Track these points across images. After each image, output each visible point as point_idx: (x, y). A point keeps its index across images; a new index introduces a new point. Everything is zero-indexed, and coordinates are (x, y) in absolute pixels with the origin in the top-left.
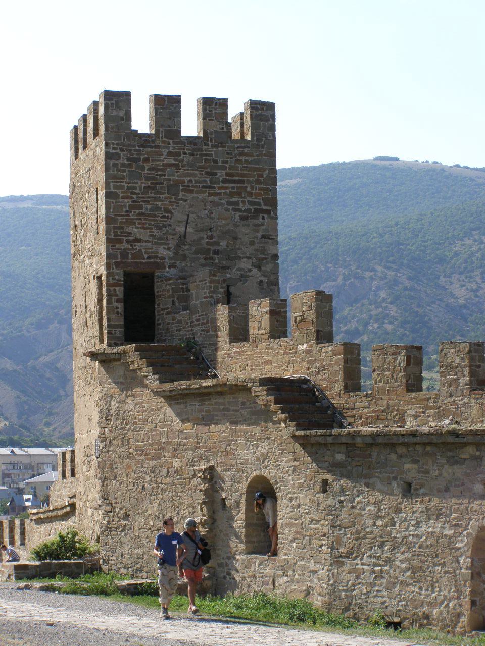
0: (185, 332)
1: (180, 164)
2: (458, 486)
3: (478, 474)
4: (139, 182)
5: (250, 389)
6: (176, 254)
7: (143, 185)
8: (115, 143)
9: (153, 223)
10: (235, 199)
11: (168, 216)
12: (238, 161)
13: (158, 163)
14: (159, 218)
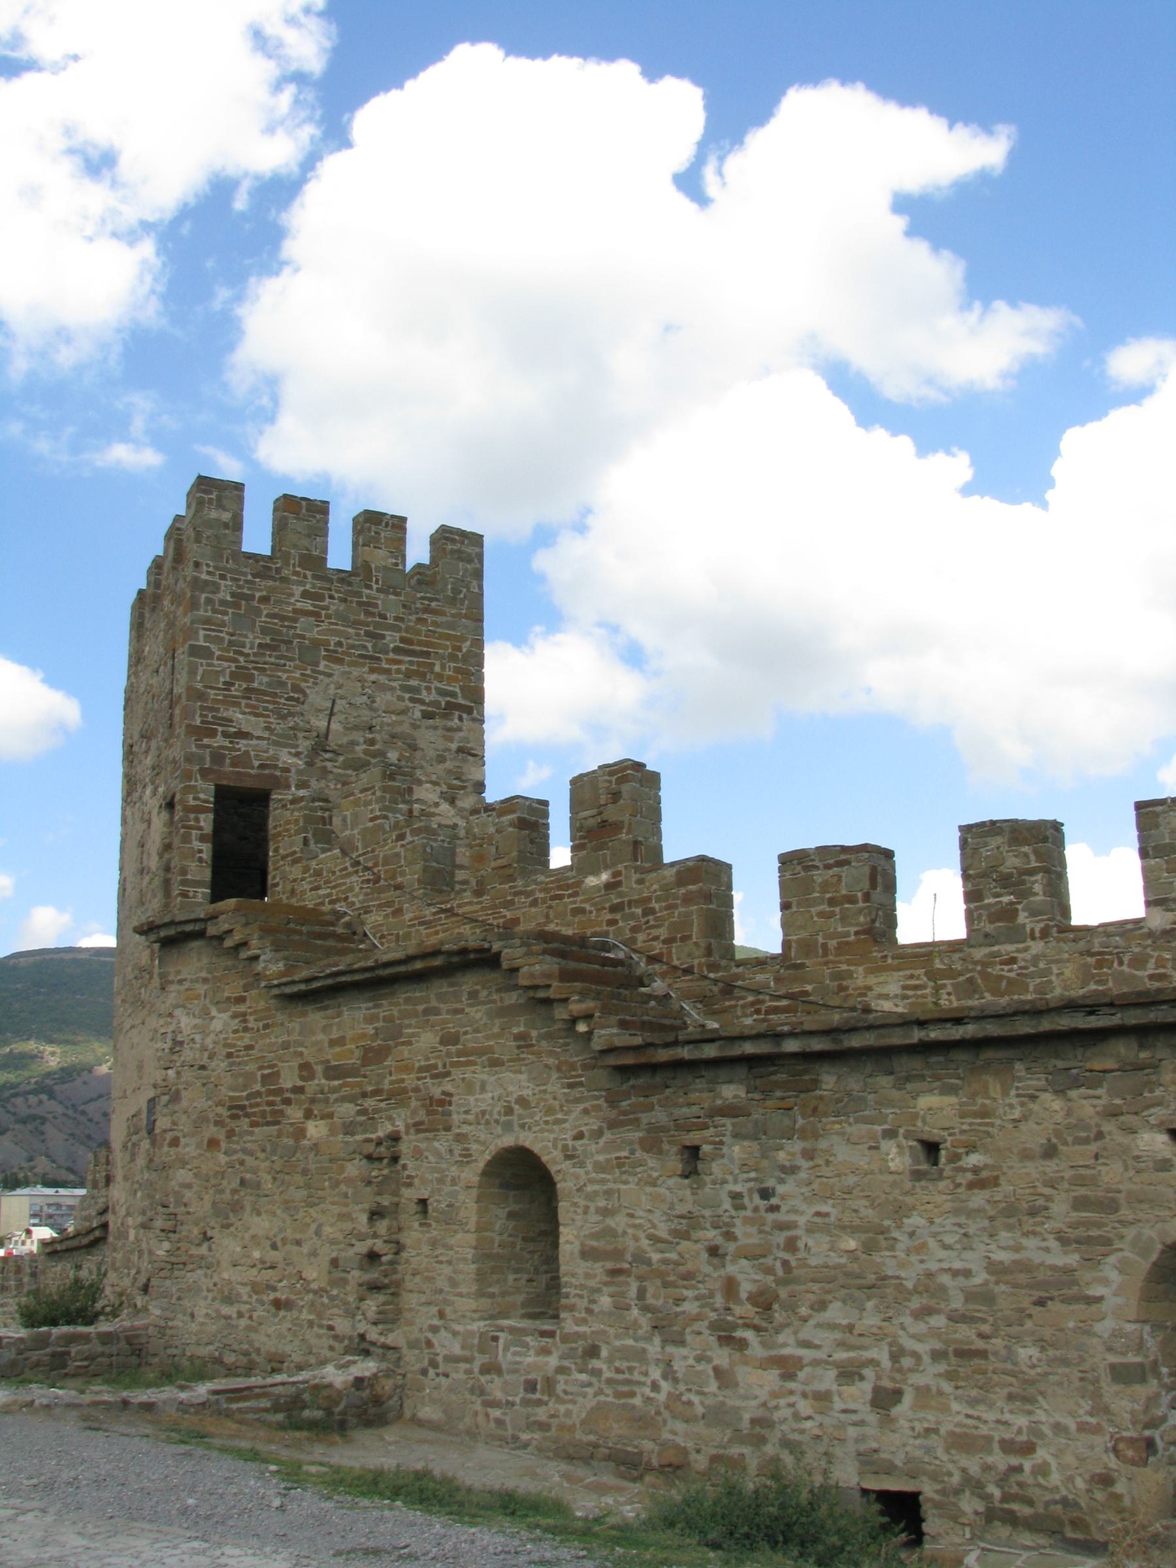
0: (329, 891)
1: (323, 612)
2: (1086, 1141)
3: (1148, 1107)
4: (251, 636)
5: (498, 955)
6: (310, 764)
7: (258, 641)
8: (211, 564)
9: (271, 707)
10: (414, 682)
12: (419, 620)
13: (284, 606)
14: (283, 701)
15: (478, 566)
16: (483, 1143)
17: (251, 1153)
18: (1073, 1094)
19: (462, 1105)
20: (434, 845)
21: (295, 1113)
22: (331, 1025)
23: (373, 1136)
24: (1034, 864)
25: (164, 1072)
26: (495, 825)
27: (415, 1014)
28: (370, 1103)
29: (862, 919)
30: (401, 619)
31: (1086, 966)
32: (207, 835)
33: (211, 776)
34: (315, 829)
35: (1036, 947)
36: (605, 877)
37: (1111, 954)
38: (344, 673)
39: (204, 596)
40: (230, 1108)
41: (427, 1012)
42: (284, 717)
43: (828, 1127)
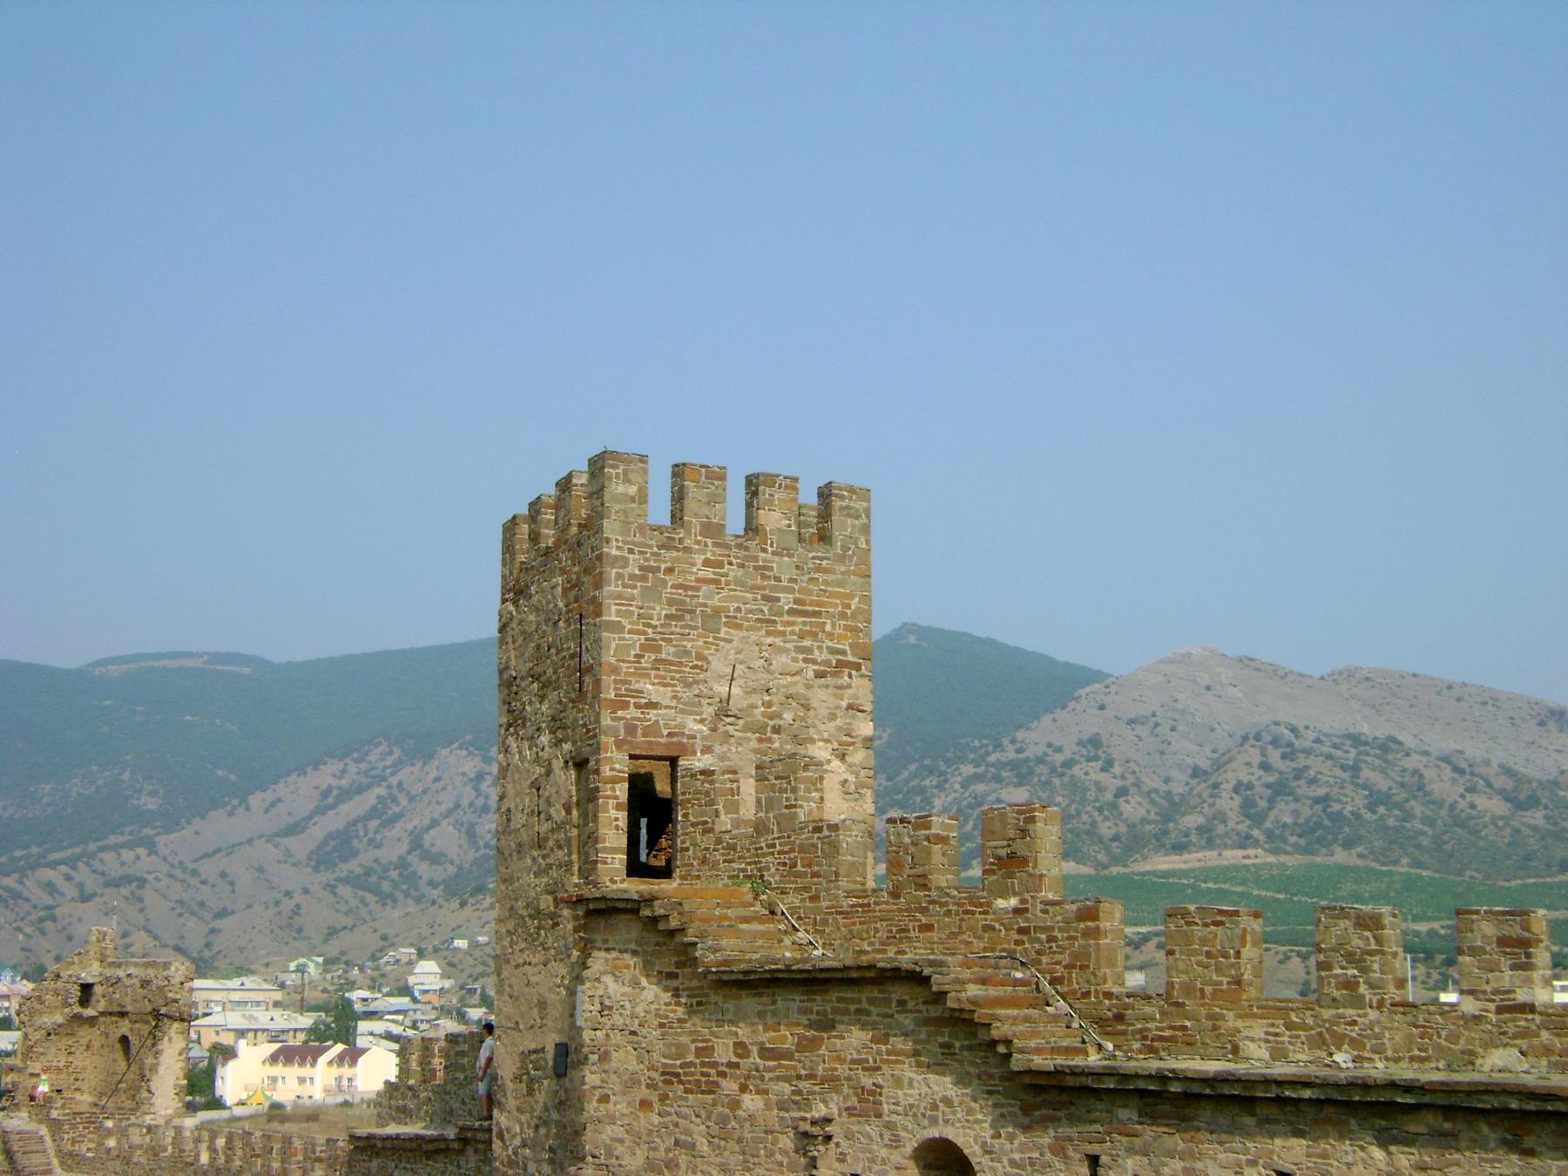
3: (1448, 1166)
4: (658, 608)
5: (928, 979)
6: (714, 730)
7: (664, 613)
9: (678, 676)
10: (807, 643)
11: (702, 666)
12: (812, 580)
14: (688, 669)
15: (866, 521)
16: (911, 1132)
17: (685, 1117)
18: (1393, 1148)
19: (892, 1097)
20: (849, 839)
21: (730, 1086)
22: (766, 1012)
23: (808, 1115)
24: (1374, 947)
25: (593, 1032)
26: (910, 836)
27: (846, 1012)
28: (805, 1085)
29: (1233, 972)
31: (1410, 1035)
32: (623, 803)
33: (625, 747)
34: (726, 800)
35: (1373, 1015)
36: (1014, 902)
37: (1431, 1028)
38: (743, 638)
39: (614, 571)
40: (663, 1073)
41: (858, 1011)
42: (689, 686)
43: (1204, 1151)
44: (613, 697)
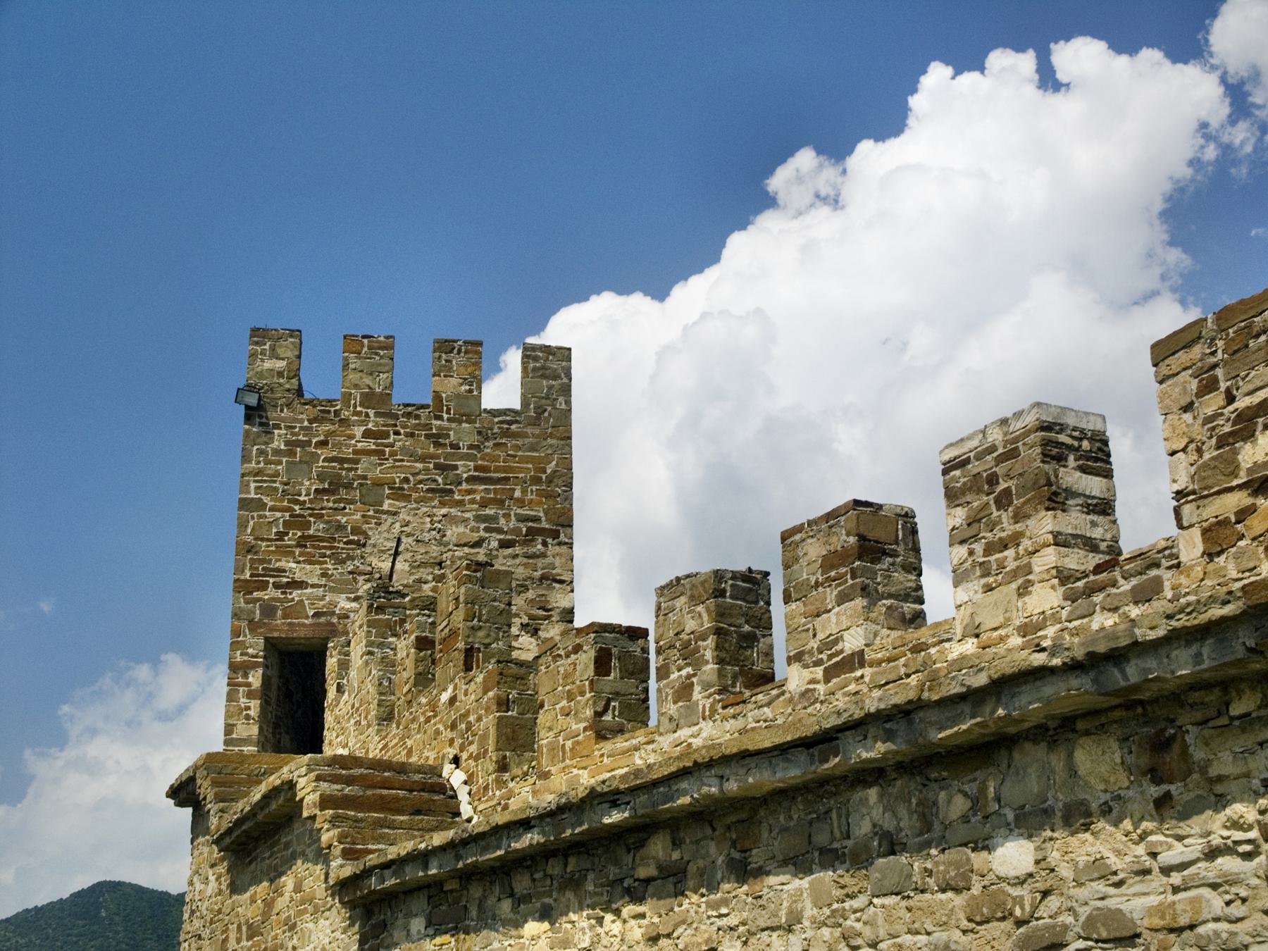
9: (328, 553)
10: (489, 511)
11: (359, 540)
14: (341, 545)
15: (565, 380)
30: (477, 447)
38: (411, 509)
39: (256, 447)
42: (343, 562)
44: (248, 576)
